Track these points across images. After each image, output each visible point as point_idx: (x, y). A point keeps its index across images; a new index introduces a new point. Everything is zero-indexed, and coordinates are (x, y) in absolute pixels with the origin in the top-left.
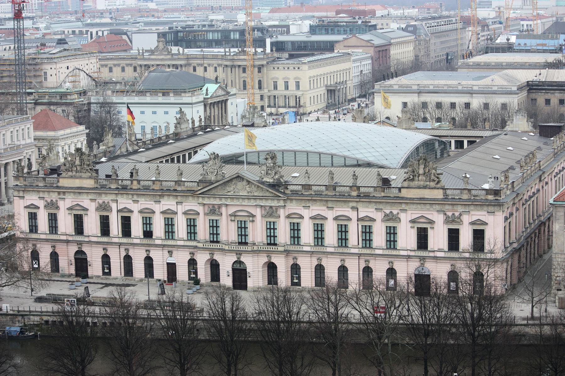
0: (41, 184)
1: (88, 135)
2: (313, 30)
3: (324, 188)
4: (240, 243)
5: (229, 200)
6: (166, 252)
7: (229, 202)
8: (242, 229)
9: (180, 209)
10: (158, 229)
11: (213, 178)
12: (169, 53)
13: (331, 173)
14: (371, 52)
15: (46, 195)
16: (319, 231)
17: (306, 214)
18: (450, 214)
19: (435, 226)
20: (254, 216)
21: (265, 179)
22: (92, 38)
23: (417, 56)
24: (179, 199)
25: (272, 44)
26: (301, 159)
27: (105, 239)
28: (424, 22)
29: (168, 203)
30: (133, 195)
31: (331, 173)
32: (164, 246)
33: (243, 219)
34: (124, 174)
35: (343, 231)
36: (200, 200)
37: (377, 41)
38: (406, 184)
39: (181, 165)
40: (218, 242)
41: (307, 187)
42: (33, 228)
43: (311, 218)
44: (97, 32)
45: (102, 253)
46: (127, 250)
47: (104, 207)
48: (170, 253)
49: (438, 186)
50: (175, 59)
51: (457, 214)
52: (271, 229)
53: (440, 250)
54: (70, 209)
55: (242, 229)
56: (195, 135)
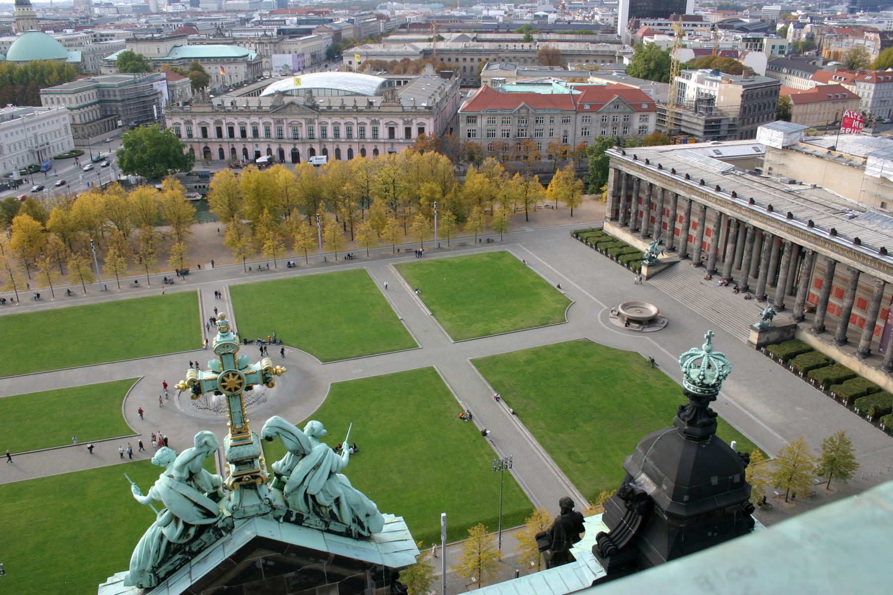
1: (192, 83)
2: (300, 22)
4: (295, 139)
7: (287, 117)
8: (295, 131)
9: (261, 122)
10: (249, 133)
12: (224, 36)
13: (342, 100)
14: (332, 34)
15: (184, 117)
17: (329, 121)
18: (406, 119)
20: (301, 124)
21: (307, 104)
27: (220, 140)
29: (255, 119)
31: (342, 100)
34: (228, 104)
35: (349, 131)
37: (335, 29)
38: (382, 105)
41: (330, 107)
43: (332, 124)
46: (233, 145)
47: (218, 122)
48: (257, 146)
52: (311, 131)
53: (401, 139)
54: (199, 124)
55: (295, 131)
56: (257, 82)
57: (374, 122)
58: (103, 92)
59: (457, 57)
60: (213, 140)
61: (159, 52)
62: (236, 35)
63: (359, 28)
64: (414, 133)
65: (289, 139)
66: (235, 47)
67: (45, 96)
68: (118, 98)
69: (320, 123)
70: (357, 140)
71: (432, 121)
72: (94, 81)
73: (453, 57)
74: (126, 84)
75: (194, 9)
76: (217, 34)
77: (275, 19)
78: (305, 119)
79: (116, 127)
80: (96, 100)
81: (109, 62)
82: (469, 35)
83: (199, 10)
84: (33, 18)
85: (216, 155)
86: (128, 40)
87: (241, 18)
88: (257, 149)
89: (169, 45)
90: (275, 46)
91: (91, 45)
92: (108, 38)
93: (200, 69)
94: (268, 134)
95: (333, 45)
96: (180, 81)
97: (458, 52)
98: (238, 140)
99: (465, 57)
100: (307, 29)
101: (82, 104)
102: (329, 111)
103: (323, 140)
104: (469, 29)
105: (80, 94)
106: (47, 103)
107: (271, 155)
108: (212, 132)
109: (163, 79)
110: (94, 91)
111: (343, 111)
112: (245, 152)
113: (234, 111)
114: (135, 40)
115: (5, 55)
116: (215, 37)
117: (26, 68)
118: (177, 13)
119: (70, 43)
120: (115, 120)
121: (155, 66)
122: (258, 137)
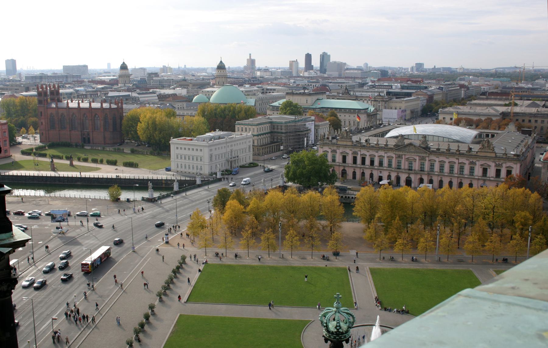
0: (330, 143)
3: (445, 150)
4: (409, 170)
5: (406, 153)
6: (379, 172)
7: (406, 154)
10: (376, 163)
11: (400, 144)
14: (427, 97)
15: (332, 147)
16: (442, 167)
17: (437, 160)
19: (491, 167)
20: (416, 160)
21: (421, 146)
22: (314, 88)
23: (443, 99)
24: (386, 151)
26: (436, 139)
27: (354, 165)
28: (446, 86)
29: (382, 153)
30: (367, 149)
31: (449, 145)
32: (378, 169)
33: (411, 161)
34: (363, 141)
35: (452, 168)
36: (395, 152)
37: (429, 93)
38: (480, 150)
39: (379, 138)
40: (400, 169)
41: (438, 149)
42: (334, 160)
44: (316, 85)
45: (353, 170)
46: (363, 170)
47: (355, 153)
48: (381, 172)
49: (493, 152)
50: (352, 97)
51: (500, 163)
52: (422, 165)
57: (472, 163)
58: (274, 126)
59: (530, 119)
60: (350, 165)
61: (307, 102)
62: (358, 94)
63: (447, 94)
64: (503, 173)
65: (405, 169)
66: (361, 102)
67: (238, 126)
68: (283, 131)
69: (430, 160)
70: (457, 175)
71: (519, 165)
72: (269, 118)
73: (527, 119)
74: (289, 122)
75: (322, 74)
76: (345, 92)
77: (385, 84)
78: (419, 156)
79: (279, 150)
80: (269, 131)
81: (273, 107)
82: (538, 102)
83: (326, 75)
84: (226, 77)
85: (350, 176)
86: (287, 94)
87: (359, 82)
88: (381, 175)
89: (315, 98)
90: (385, 103)
91: (261, 95)
92: (271, 91)
93: (336, 116)
94: (390, 165)
95: (427, 105)
96: (323, 123)
97: (531, 115)
98: (367, 167)
99: (536, 119)
100: (408, 93)
101: (260, 133)
102: (438, 152)
103: (431, 173)
104: (538, 97)
105: (260, 126)
107: (390, 180)
108: (349, 160)
109: (313, 121)
110: (268, 125)
111: (448, 153)
112: (371, 176)
113: (367, 146)
114: (293, 94)
115: (209, 99)
116: (343, 94)
117: (225, 108)
118: (312, 77)
119: (248, 93)
120: (279, 146)
121: (304, 112)
122: (382, 166)
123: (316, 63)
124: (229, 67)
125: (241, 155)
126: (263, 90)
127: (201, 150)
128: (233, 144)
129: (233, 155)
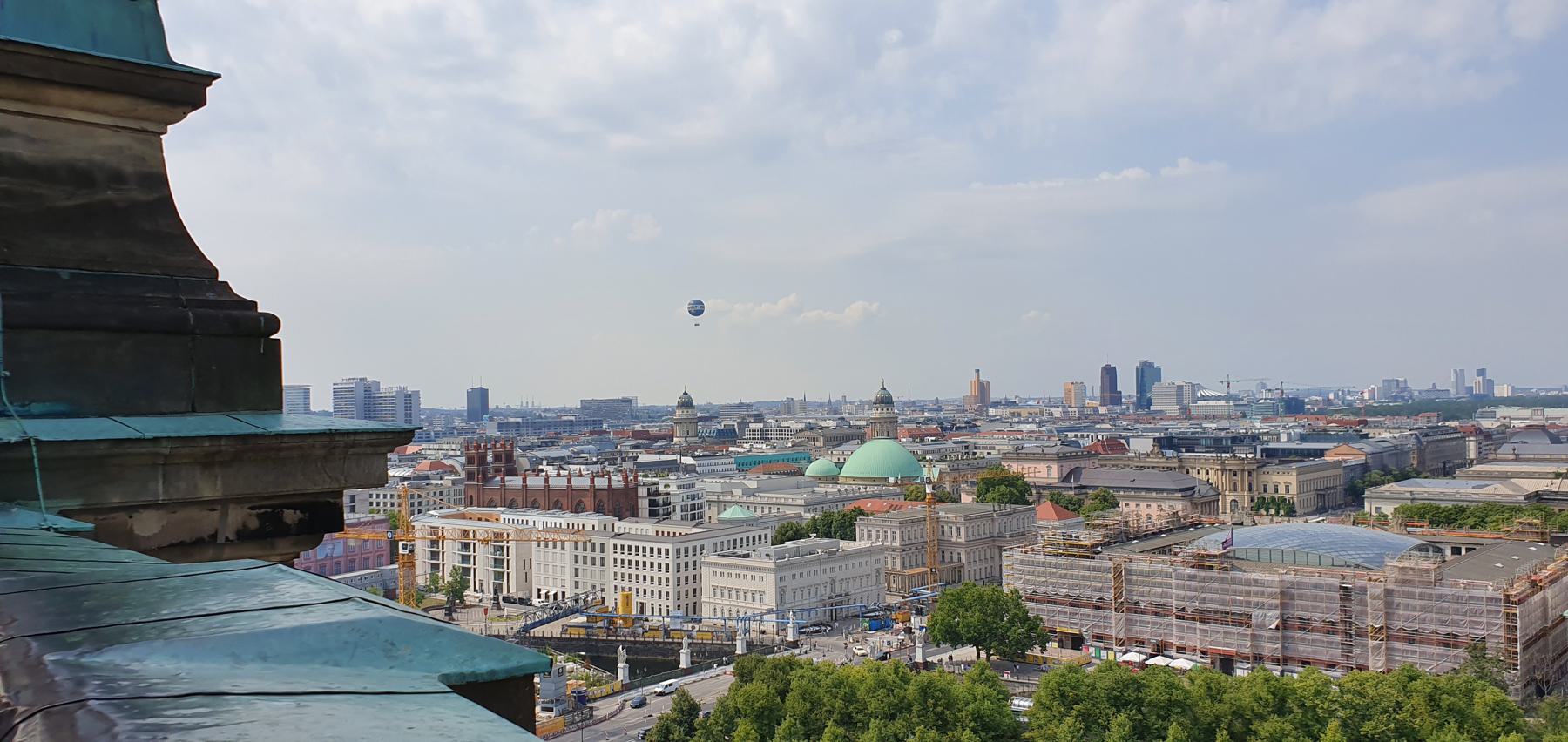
25: (1262, 449)
106: (862, 535)
115: (841, 469)
123: (1127, 385)
124: (937, 398)
125: (857, 591)
126: (967, 448)
127: (761, 578)
128: (837, 565)
129: (838, 591)
